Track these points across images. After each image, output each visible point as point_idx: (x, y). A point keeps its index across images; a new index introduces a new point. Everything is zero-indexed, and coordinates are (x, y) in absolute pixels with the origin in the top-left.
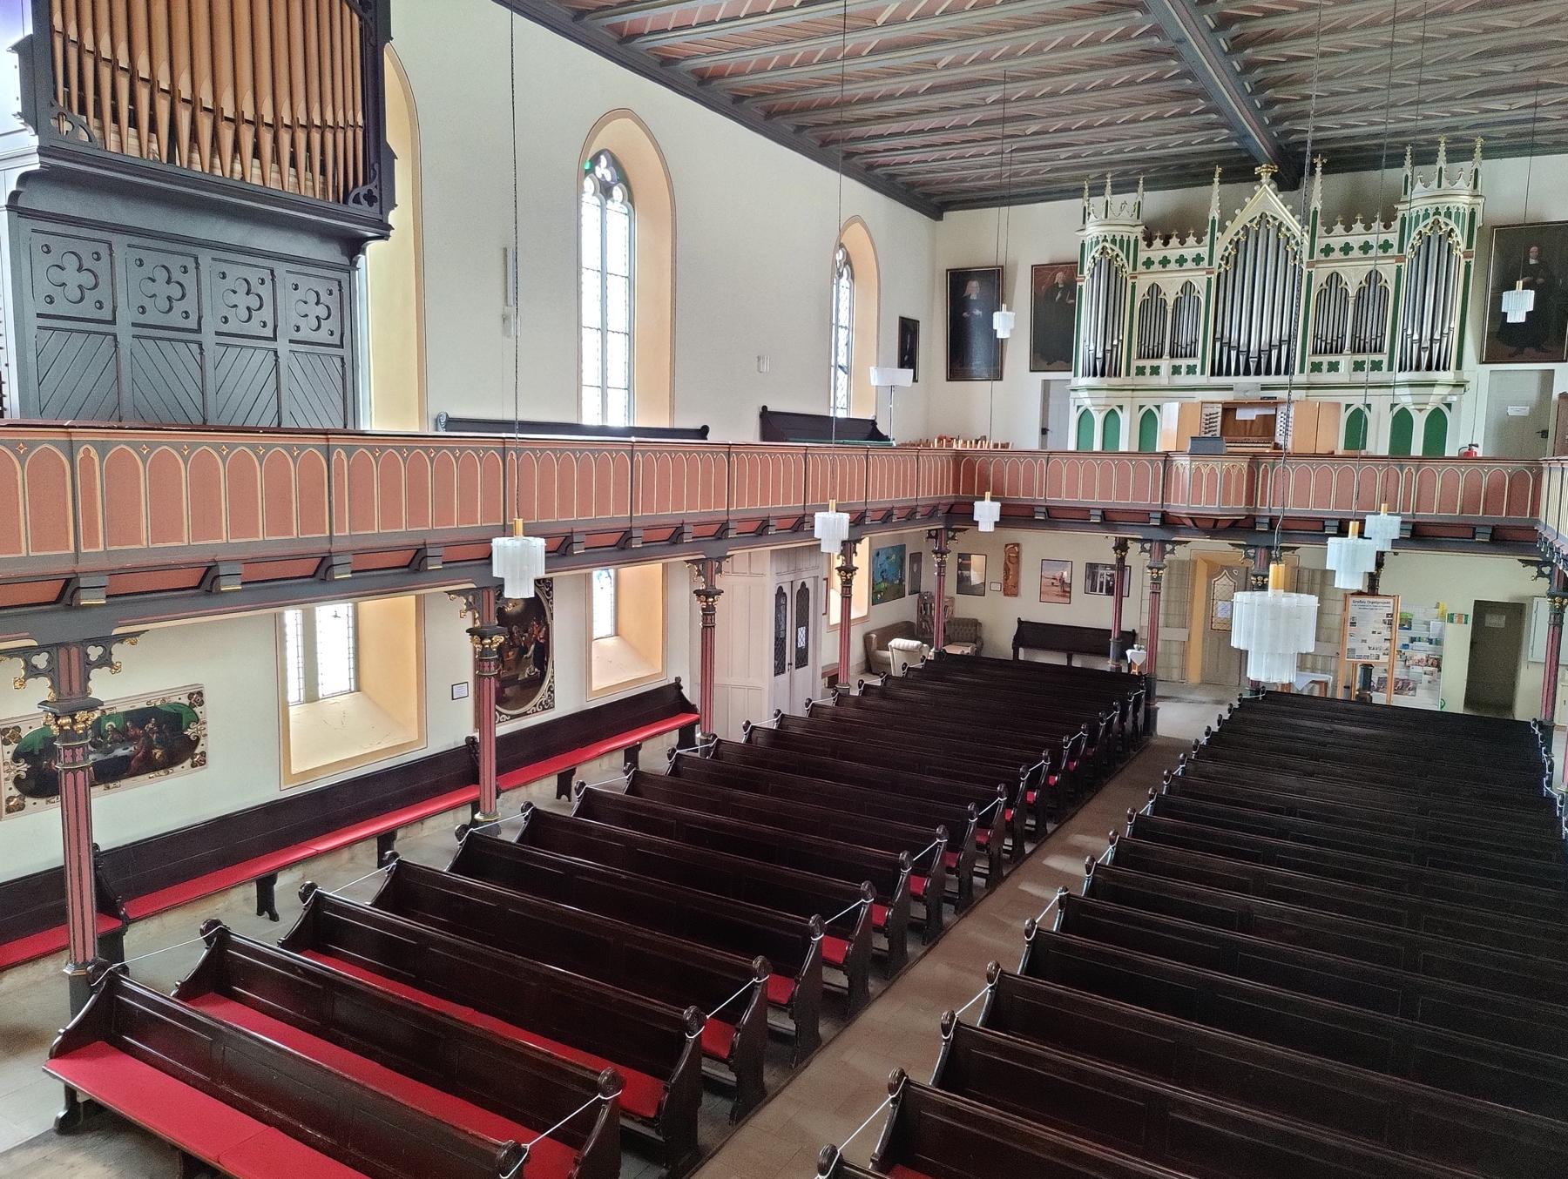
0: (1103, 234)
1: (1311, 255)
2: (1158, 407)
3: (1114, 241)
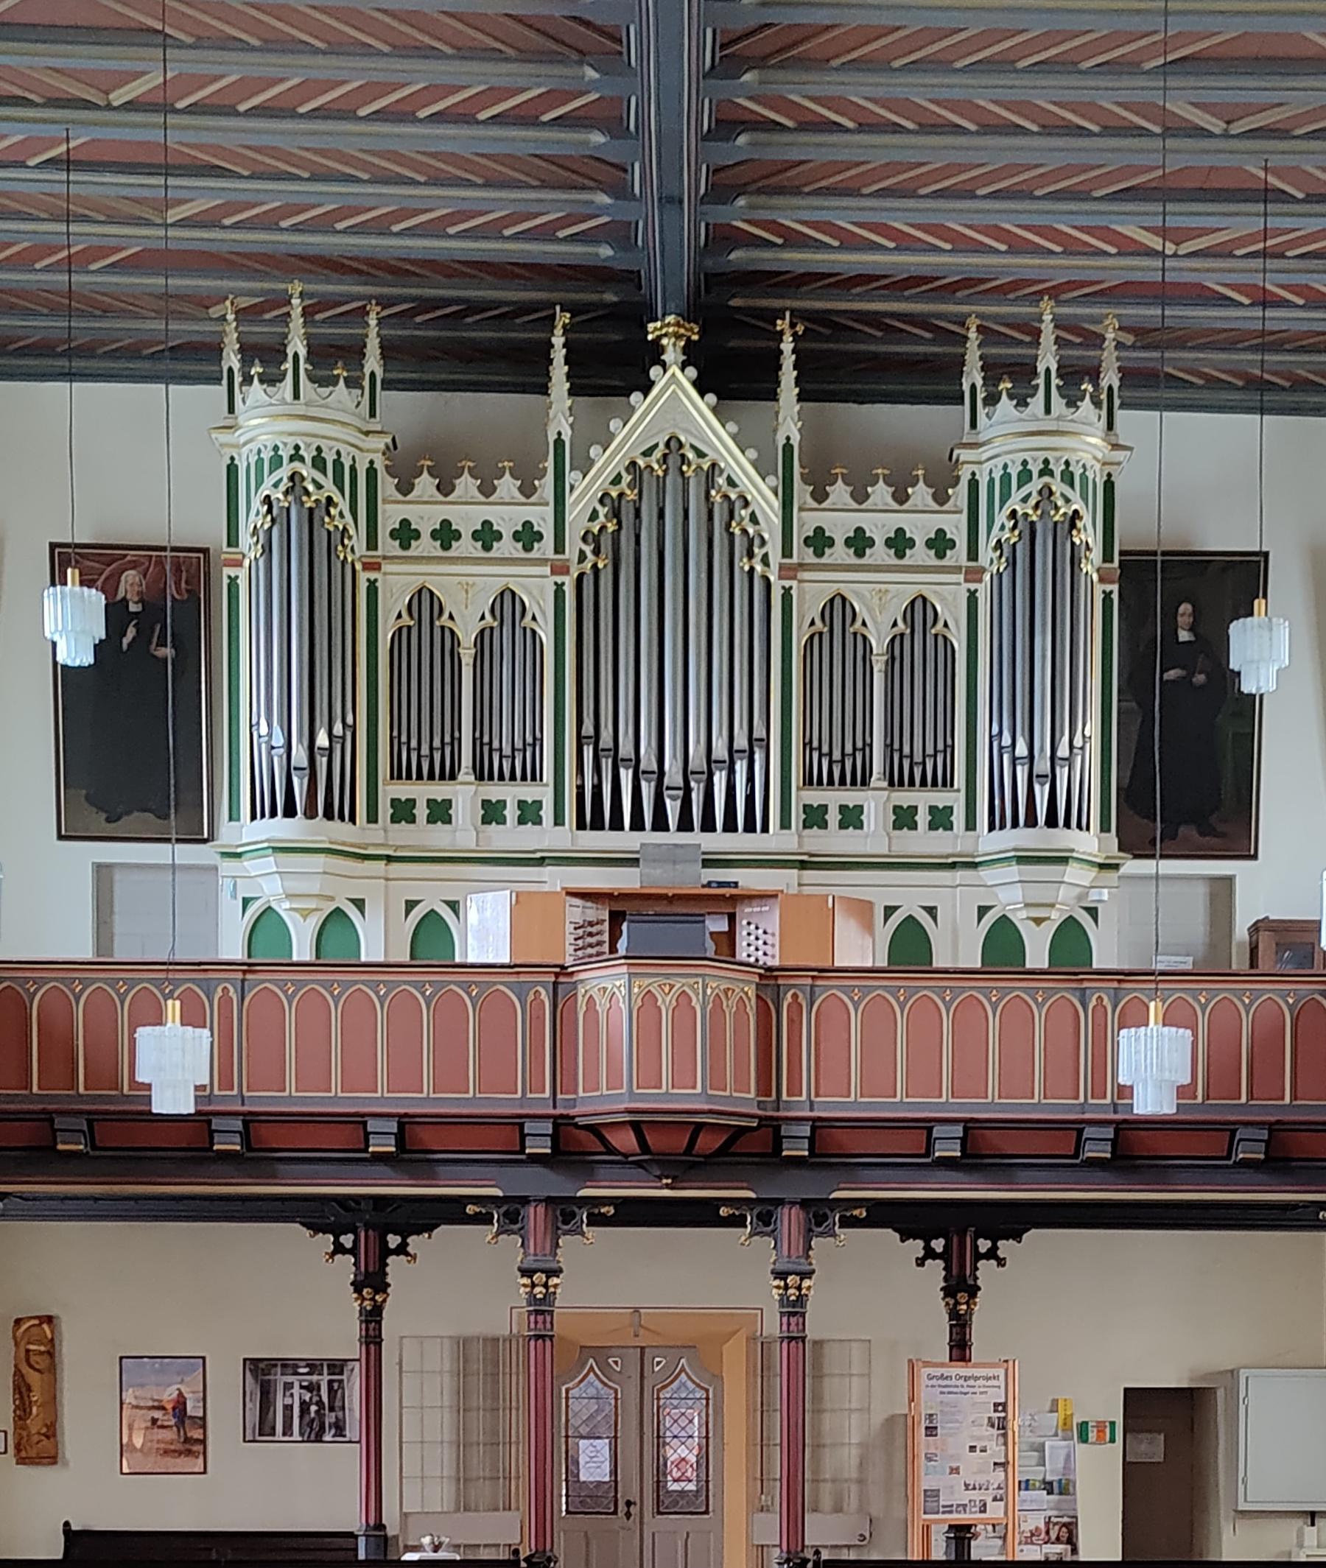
0: (291, 441)
1: (787, 552)
2: (453, 906)
3: (319, 463)
